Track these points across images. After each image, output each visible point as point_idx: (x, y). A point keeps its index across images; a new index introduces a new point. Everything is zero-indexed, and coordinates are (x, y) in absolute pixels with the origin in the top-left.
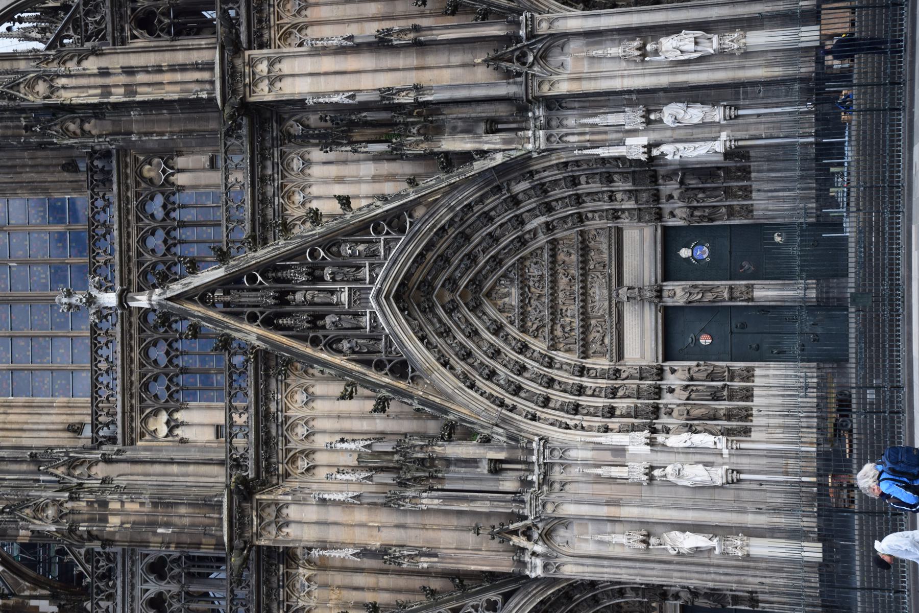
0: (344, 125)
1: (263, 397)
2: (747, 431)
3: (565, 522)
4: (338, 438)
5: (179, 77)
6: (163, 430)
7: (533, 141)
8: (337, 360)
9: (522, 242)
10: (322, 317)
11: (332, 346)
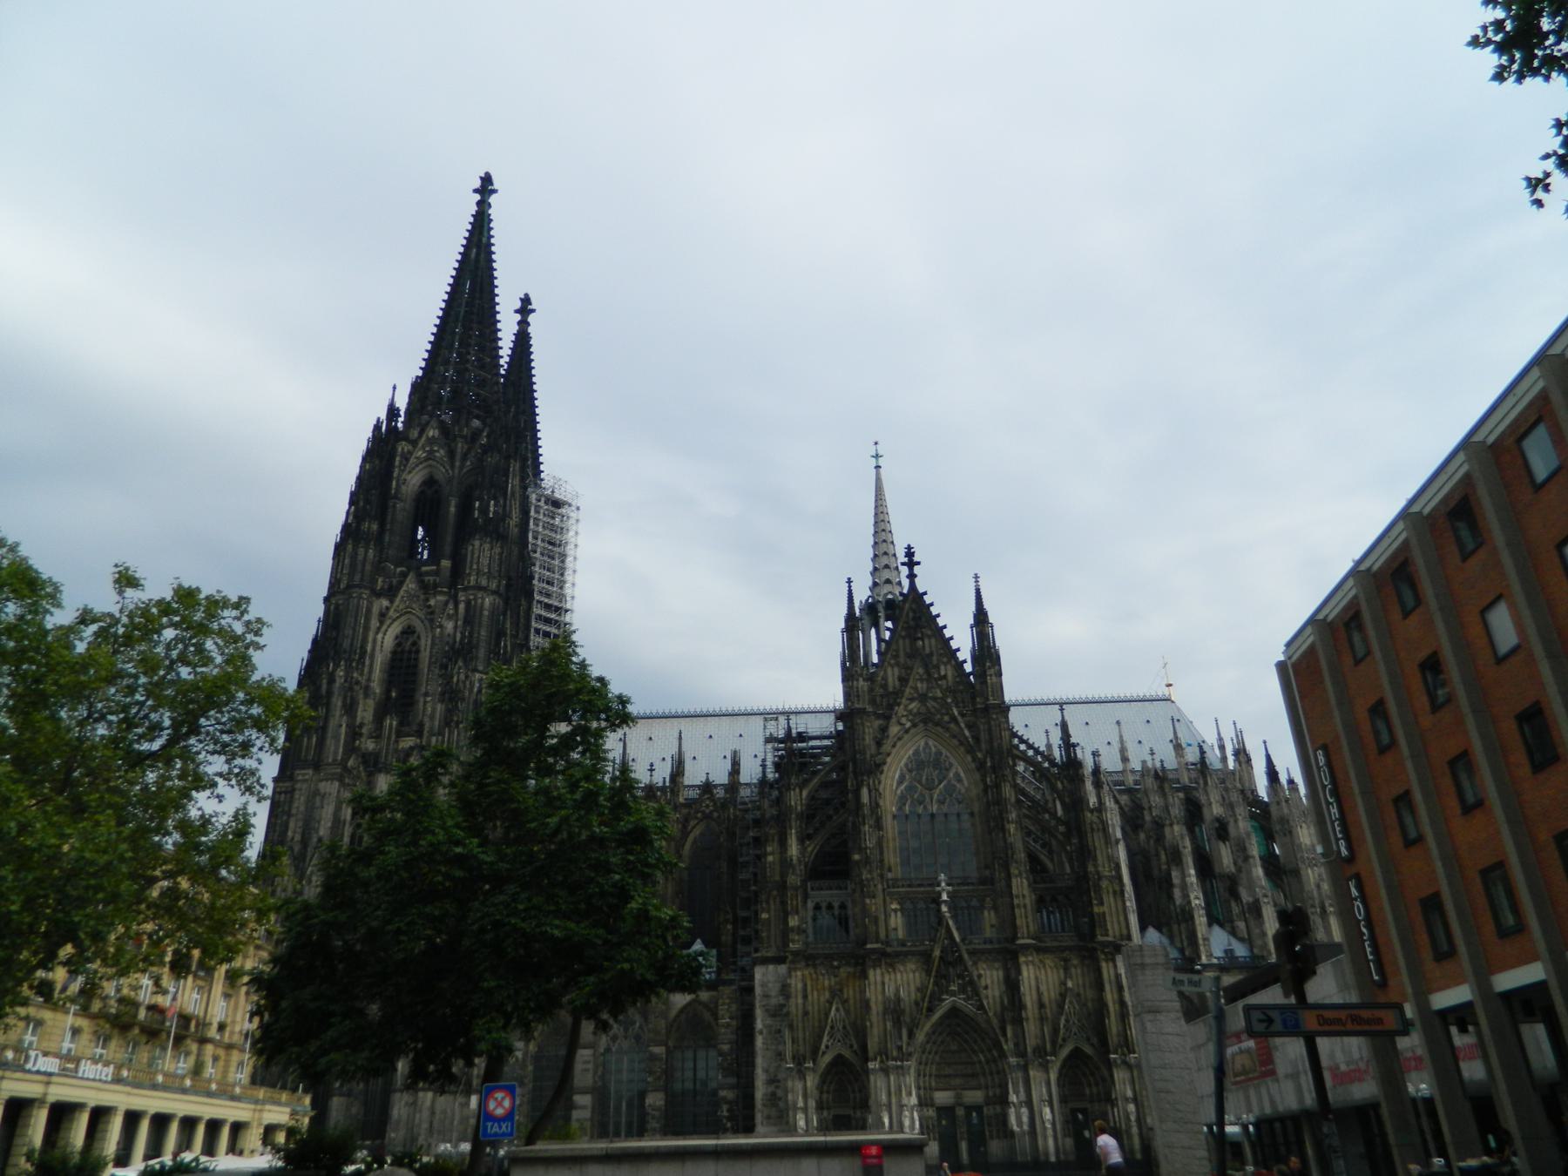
0: (1012, 985)
1: (913, 954)
7: (1013, 1060)
9: (974, 1052)
11: (936, 983)
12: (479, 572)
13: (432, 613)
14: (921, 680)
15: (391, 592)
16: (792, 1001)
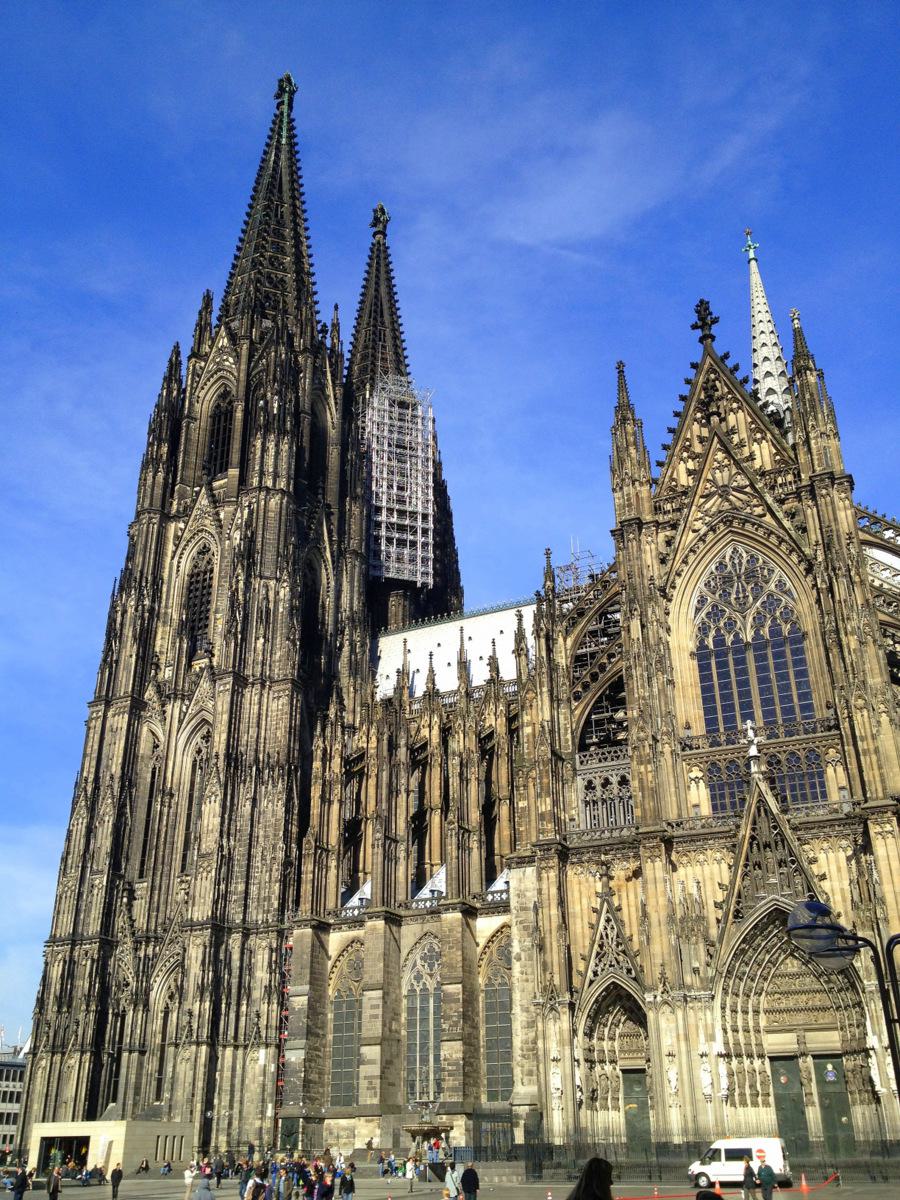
1: (714, 836)
2: (733, 1104)
3: (673, 1012)
4: (701, 880)
5: (878, 779)
6: (693, 775)
8: (739, 879)
10: (760, 868)
11: (745, 875)
12: (262, 474)
13: (221, 527)
14: (721, 468)
15: (184, 514)
16: (546, 910)
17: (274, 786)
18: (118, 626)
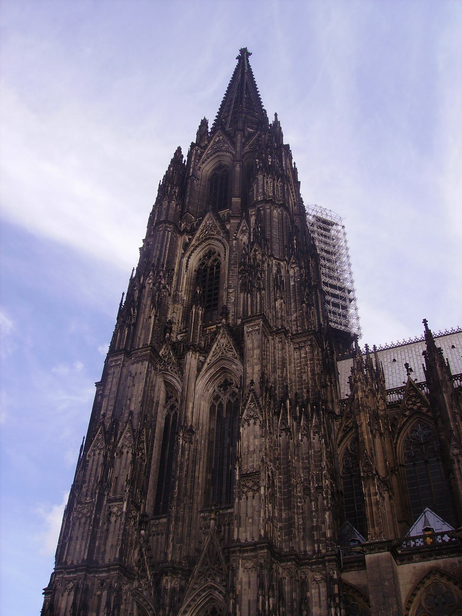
17: (308, 420)
18: (136, 299)
